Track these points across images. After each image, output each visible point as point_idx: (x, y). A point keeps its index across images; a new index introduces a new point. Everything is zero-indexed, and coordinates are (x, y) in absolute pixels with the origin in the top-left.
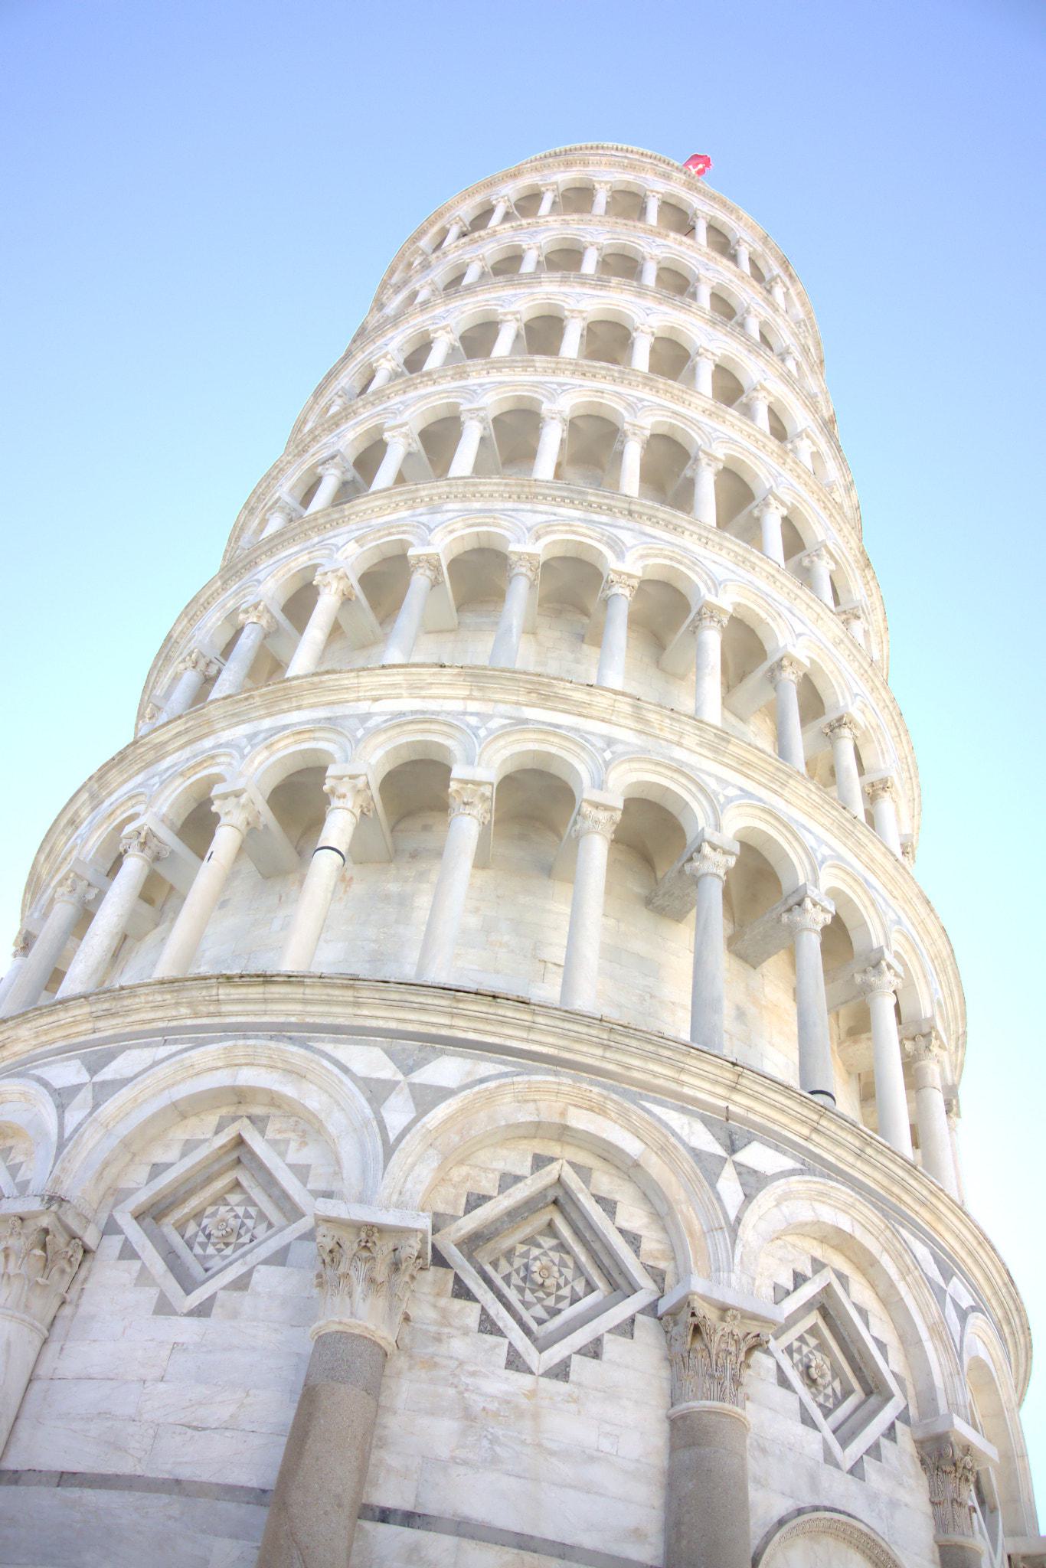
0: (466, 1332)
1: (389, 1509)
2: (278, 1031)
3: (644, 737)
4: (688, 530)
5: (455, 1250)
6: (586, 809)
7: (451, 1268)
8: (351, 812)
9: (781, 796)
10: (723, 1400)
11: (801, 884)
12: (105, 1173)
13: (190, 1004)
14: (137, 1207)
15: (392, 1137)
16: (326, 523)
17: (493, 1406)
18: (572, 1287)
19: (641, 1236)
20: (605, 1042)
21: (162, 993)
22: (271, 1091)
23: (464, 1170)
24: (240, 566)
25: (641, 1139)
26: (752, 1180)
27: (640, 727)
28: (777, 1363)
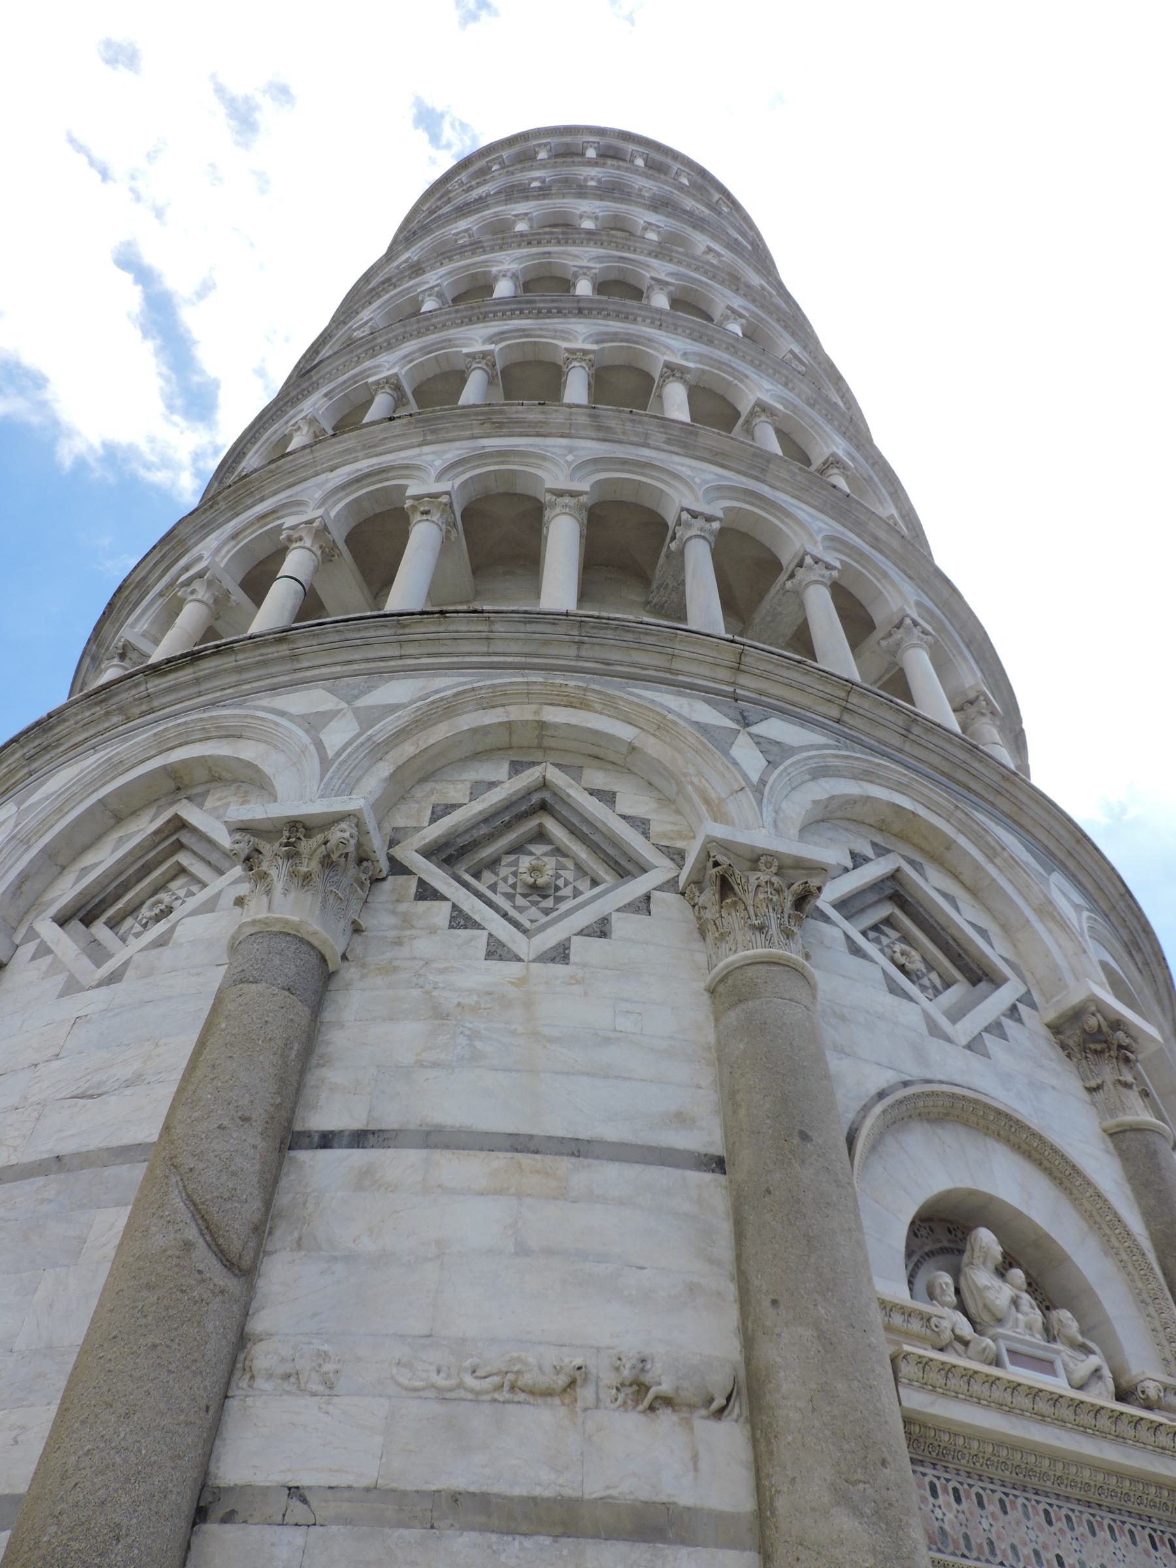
0: (433, 930)
1: (331, 1132)
3: (607, 443)
4: (640, 316)
7: (415, 874)
8: (310, 550)
9: (763, 482)
12: (24, 888)
13: (121, 710)
14: (59, 911)
19: (649, 820)
21: (89, 708)
22: (203, 757)
24: (230, 461)
25: (634, 725)
26: (775, 749)
27: (601, 435)
28: (845, 933)
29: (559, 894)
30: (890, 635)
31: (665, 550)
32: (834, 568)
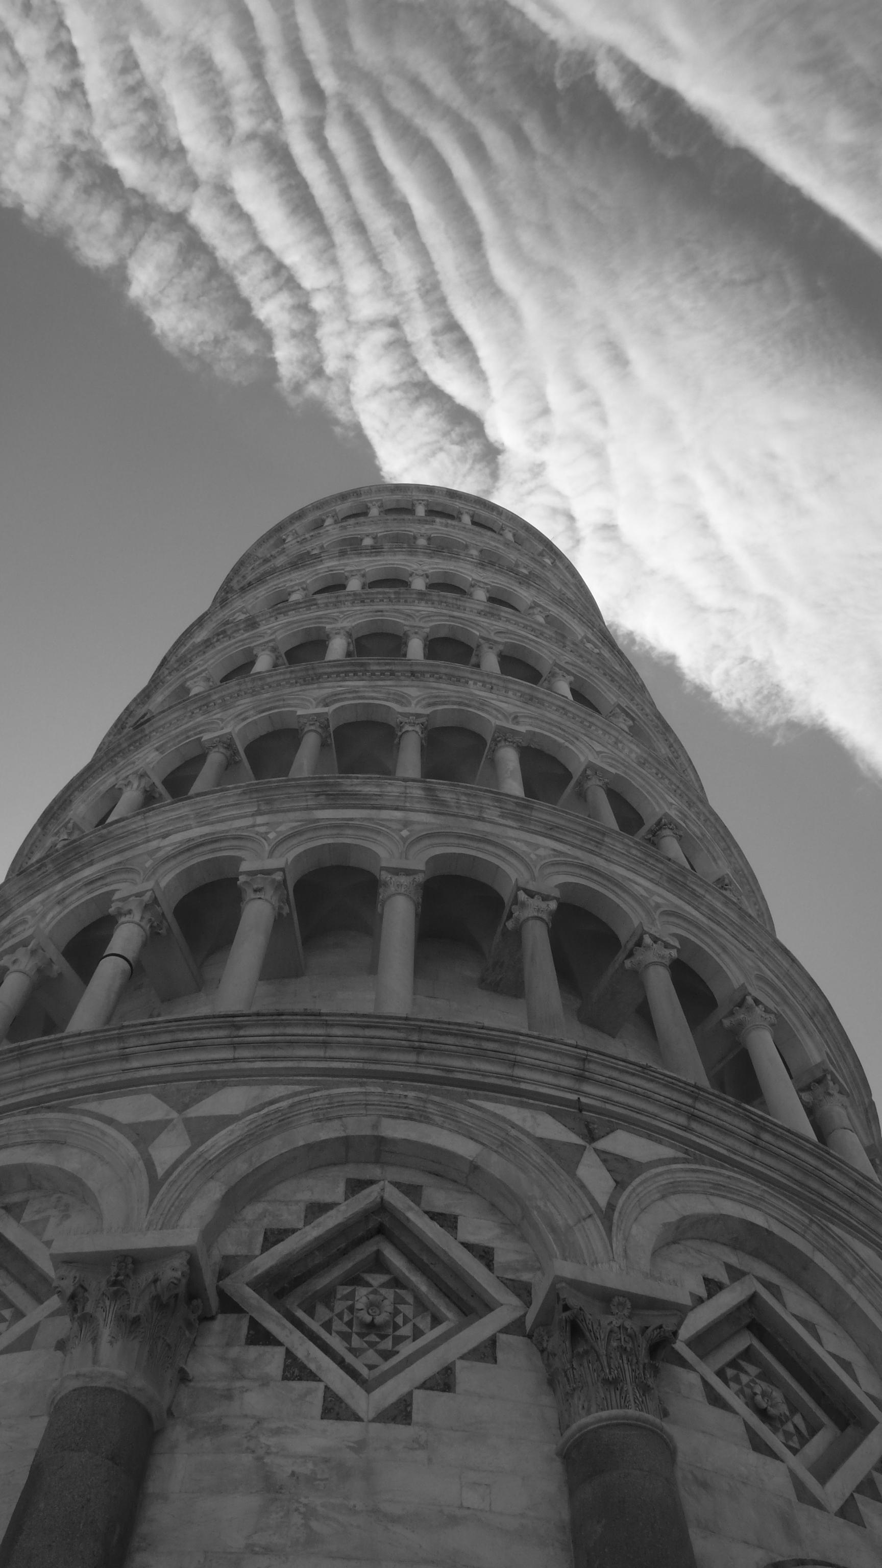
0: (265, 1382)
2: (37, 1105)
3: (442, 817)
4: (471, 679)
5: (249, 1292)
6: (385, 876)
8: (139, 925)
9: (599, 855)
10: (627, 1407)
11: (636, 926)
15: (160, 1172)
16: (130, 746)
17: (306, 1469)
18: (414, 1325)
19: (493, 1249)
20: (417, 1044)
23: (259, 1207)
25: (476, 1141)
27: (436, 808)
29: (398, 1333)
30: (732, 1013)
31: (500, 929)
32: (673, 947)
